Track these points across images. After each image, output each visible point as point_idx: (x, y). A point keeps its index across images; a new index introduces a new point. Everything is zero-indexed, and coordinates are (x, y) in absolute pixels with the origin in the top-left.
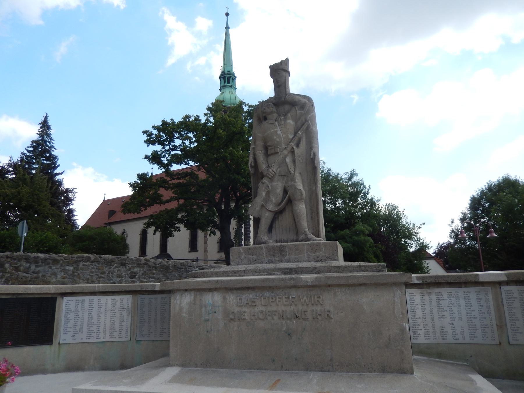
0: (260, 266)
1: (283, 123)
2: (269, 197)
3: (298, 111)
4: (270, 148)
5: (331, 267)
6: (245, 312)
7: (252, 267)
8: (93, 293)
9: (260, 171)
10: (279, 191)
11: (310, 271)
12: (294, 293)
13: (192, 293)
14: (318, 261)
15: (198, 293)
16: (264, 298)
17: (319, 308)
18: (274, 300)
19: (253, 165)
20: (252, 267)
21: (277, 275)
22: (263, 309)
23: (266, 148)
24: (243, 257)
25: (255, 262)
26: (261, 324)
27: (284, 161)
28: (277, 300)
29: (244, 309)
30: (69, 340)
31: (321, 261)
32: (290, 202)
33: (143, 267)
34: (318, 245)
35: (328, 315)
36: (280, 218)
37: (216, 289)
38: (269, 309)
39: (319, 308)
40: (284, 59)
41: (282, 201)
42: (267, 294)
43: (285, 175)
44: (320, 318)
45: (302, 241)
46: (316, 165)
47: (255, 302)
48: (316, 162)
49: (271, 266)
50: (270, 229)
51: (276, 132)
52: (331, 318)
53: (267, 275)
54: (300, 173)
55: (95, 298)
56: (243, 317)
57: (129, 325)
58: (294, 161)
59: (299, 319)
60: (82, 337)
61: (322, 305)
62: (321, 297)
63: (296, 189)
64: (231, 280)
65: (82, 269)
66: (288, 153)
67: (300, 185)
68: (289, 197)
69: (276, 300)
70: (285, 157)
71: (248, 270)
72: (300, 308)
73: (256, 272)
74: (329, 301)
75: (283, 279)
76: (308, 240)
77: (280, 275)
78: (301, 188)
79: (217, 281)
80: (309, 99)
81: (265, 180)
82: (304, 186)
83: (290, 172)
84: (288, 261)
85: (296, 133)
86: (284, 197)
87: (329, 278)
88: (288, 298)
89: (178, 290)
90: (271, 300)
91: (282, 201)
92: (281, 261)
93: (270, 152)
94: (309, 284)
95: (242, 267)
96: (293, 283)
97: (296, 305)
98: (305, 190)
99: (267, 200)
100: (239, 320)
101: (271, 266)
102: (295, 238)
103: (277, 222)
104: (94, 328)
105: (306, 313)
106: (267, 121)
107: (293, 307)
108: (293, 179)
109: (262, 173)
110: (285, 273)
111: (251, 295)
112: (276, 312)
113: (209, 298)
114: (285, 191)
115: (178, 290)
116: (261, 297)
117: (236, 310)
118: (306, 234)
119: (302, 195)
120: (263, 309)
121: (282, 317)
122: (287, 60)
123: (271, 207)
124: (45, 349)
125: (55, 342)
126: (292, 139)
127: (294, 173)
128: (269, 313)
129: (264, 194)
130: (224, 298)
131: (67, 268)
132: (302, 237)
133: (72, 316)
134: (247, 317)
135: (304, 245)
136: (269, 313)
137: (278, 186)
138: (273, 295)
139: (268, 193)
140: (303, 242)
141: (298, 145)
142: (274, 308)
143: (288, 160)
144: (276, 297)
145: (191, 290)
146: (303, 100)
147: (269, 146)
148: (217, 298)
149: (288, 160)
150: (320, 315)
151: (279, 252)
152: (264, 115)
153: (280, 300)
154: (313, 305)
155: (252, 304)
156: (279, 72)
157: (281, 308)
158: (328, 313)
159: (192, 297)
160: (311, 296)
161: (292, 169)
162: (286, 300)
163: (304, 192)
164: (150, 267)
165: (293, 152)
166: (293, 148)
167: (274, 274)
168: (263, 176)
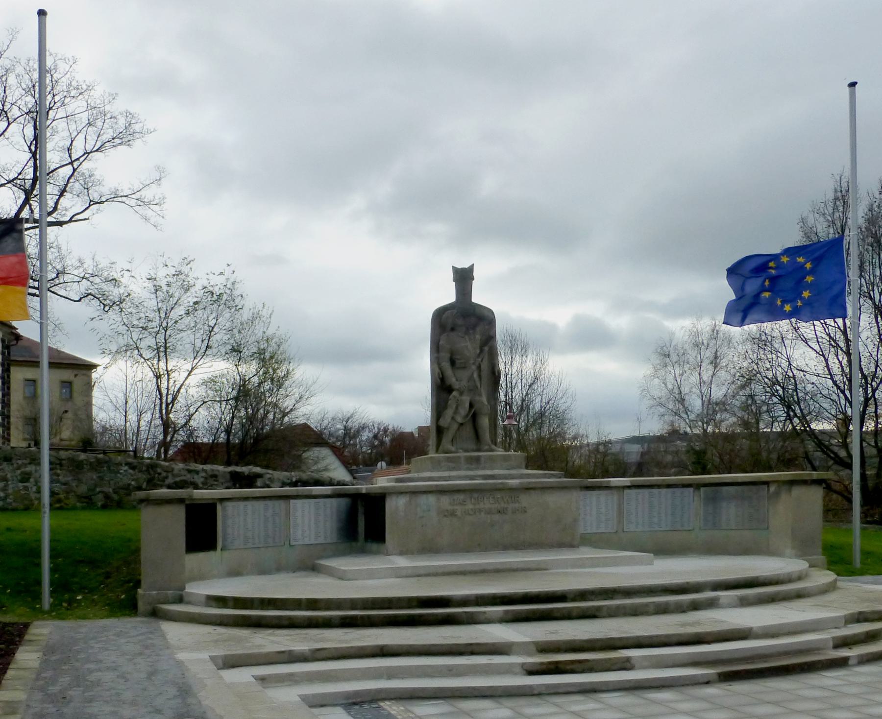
10: (467, 405)
12: (499, 495)
13: (408, 495)
20: (454, 473)
22: (471, 507)
25: (453, 469)
29: (456, 507)
37: (430, 492)
38: (477, 506)
42: (476, 495)
51: (467, 347)
58: (480, 376)
67: (484, 399)
72: (503, 505)
76: (492, 450)
81: (454, 393)
84: (484, 469)
92: (477, 469)
99: (456, 411)
107: (496, 506)
108: (480, 395)
111: (461, 497)
113: (423, 500)
114: (471, 405)
117: (450, 508)
120: (471, 507)
129: (454, 406)
132: (486, 447)
134: (459, 513)
137: (466, 399)
142: (482, 506)
143: (475, 375)
145: (406, 493)
146: (486, 313)
165: (479, 367)
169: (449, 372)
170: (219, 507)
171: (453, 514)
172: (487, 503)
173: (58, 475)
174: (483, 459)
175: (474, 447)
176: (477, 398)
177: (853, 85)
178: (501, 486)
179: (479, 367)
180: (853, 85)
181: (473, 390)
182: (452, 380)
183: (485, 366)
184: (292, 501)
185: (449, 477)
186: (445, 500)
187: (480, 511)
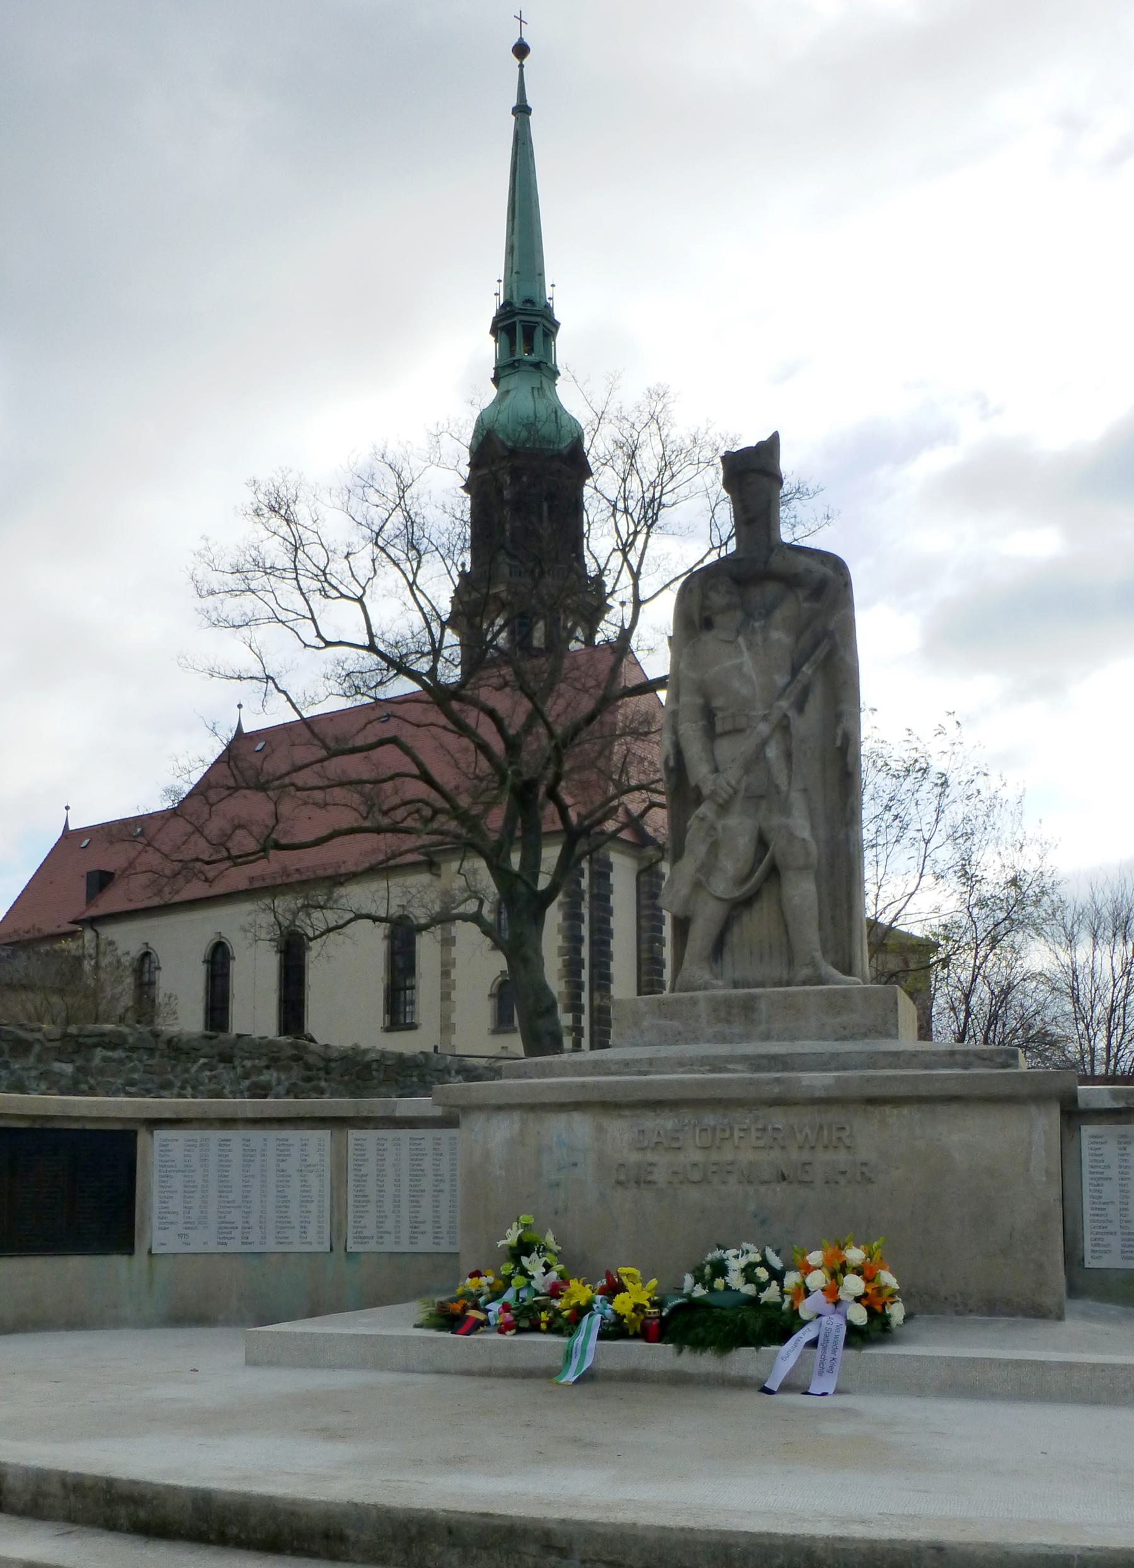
1: (759, 638)
2: (716, 857)
3: (806, 605)
4: (720, 715)
5: (878, 1053)
6: (652, 1164)
8: (227, 1122)
9: (693, 783)
10: (744, 843)
11: (823, 1063)
12: (779, 1118)
14: (843, 1038)
15: (532, 1115)
16: (702, 1130)
17: (841, 1157)
18: (727, 1135)
19: (672, 763)
21: (734, 1071)
22: (697, 1156)
23: (708, 714)
24: (645, 1024)
25: (676, 1038)
26: (694, 1195)
28: (737, 1134)
29: (651, 1157)
30: (173, 1245)
31: (852, 1037)
32: (774, 873)
33: (287, 1069)
34: (845, 994)
35: (863, 1173)
36: (745, 918)
38: (715, 1157)
39: (841, 1157)
40: (765, 437)
41: (752, 871)
42: (710, 1119)
43: (762, 797)
44: (843, 1180)
45: (804, 983)
46: (850, 768)
47: (678, 1139)
48: (850, 759)
49: (723, 1050)
50: (718, 948)
52: (870, 1181)
53: (710, 1071)
54: (805, 790)
55: (236, 1136)
56: (650, 1178)
57: (327, 1215)
58: (788, 756)
59: (791, 1183)
60: (204, 1241)
61: (849, 1148)
62: (848, 1128)
63: (791, 837)
64: (617, 1082)
65: (102, 1072)
66: (773, 731)
67: (800, 825)
68: (773, 859)
69: (732, 1135)
70: (764, 743)
71: (658, 1059)
72: (795, 1155)
73: (682, 1064)
74: (869, 1136)
75: (751, 1082)
77: (743, 1072)
80: (837, 566)
81: (704, 809)
82: (813, 828)
83: (777, 786)
84: (767, 1037)
85: (795, 670)
86: (758, 861)
87: (869, 1080)
88: (764, 1129)
89: (480, 1107)
90: (719, 1135)
91: (752, 871)
92: (746, 1037)
93: (719, 728)
94: (817, 1094)
95: (643, 1053)
96: (777, 1090)
97: (783, 1148)
98: (817, 842)
100: (637, 1182)
101: (723, 1050)
102: (785, 977)
103: (736, 930)
104: (235, 1216)
105: (807, 1168)
106: (714, 632)
109: (697, 788)
110: (758, 1068)
111: (666, 1122)
112: (732, 1163)
114: (762, 843)
115: (480, 1107)
116: (695, 1126)
118: (813, 964)
119: (808, 854)
121: (750, 1177)
122: (775, 438)
123: (722, 886)
124: (117, 1263)
125: (140, 1247)
126: (785, 689)
127: (789, 791)
128: (714, 1168)
129: (702, 850)
130: (600, 1129)
131: (57, 1066)
133: (177, 1182)
135: (808, 993)
136: (714, 1168)
138: (726, 1121)
139: (714, 847)
140: (808, 988)
142: (728, 1155)
144: (731, 1128)
147: (721, 709)
148: (581, 1126)
150: (843, 1173)
151: (741, 1012)
152: (707, 614)
153: (742, 1134)
154: (826, 1147)
156: (752, 476)
157: (747, 1156)
158: (865, 1169)
159: (517, 1126)
160: (821, 1127)
161: (782, 780)
162: (759, 1135)
163: (813, 848)
164: (308, 1067)
165: (784, 727)
166: (785, 716)
167: (728, 1071)
168: (699, 799)
169: (694, 750)
170: (142, 1138)
171: (641, 1179)
174: (763, 1006)
175: (781, 972)
176: (776, 820)
178: (776, 1090)
179: (784, 727)
181: (763, 796)
182: (699, 771)
183: (806, 725)
184: (353, 1134)
185: (651, 1062)
186: (620, 1131)
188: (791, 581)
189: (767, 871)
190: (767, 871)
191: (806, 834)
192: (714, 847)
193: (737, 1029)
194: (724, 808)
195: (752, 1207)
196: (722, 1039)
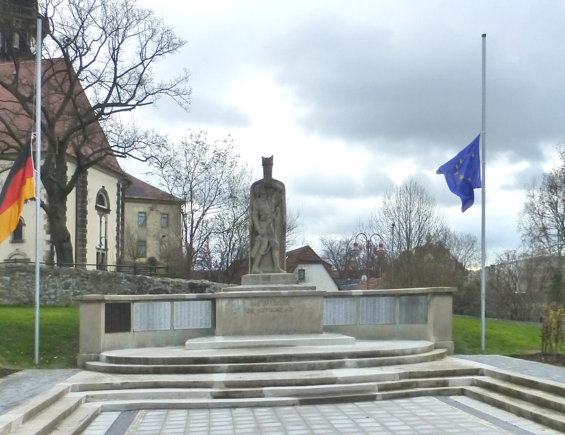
0: (259, 286)
7: (254, 286)
10: (266, 243)
12: (277, 300)
20: (254, 286)
22: (262, 307)
25: (255, 284)
26: (261, 314)
27: (269, 226)
29: (253, 307)
42: (265, 300)
50: (259, 265)
58: (274, 226)
63: (275, 242)
67: (277, 241)
78: (277, 242)
79: (242, 294)
84: (272, 283)
92: (268, 284)
99: (259, 248)
108: (274, 237)
111: (256, 301)
114: (269, 243)
117: (250, 307)
120: (262, 307)
121: (272, 311)
123: (262, 252)
129: (258, 245)
134: (255, 311)
137: (265, 240)
139: (260, 245)
141: (276, 216)
142: (268, 307)
143: (271, 225)
146: (278, 185)
148: (240, 302)
149: (271, 225)
151: (267, 279)
155: (257, 305)
161: (273, 231)
165: (274, 220)
171: (251, 311)
172: (271, 305)
173: (86, 285)
174: (272, 278)
177: (484, 36)
178: (278, 294)
179: (274, 220)
180: (484, 36)
181: (270, 234)
183: (278, 219)
187: (267, 309)
188: (276, 189)
189: (270, 250)
190: (270, 250)
191: (277, 242)
192: (260, 245)
193: (267, 282)
194: (263, 237)
195: (272, 316)
196: (264, 284)
